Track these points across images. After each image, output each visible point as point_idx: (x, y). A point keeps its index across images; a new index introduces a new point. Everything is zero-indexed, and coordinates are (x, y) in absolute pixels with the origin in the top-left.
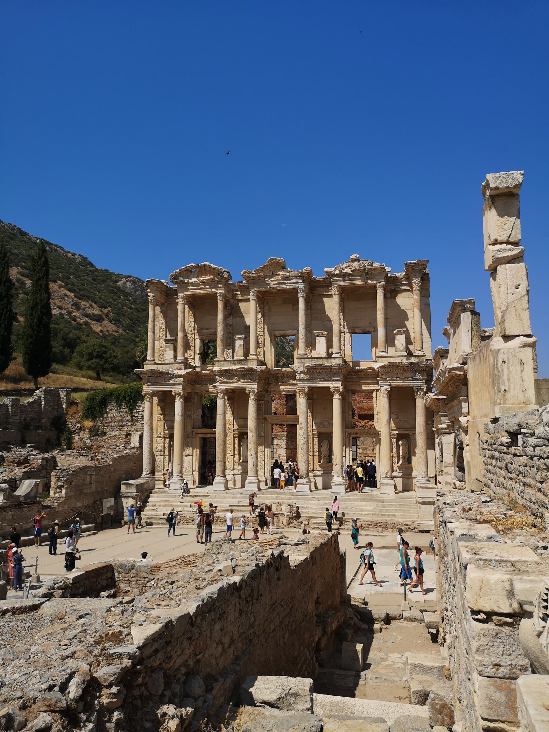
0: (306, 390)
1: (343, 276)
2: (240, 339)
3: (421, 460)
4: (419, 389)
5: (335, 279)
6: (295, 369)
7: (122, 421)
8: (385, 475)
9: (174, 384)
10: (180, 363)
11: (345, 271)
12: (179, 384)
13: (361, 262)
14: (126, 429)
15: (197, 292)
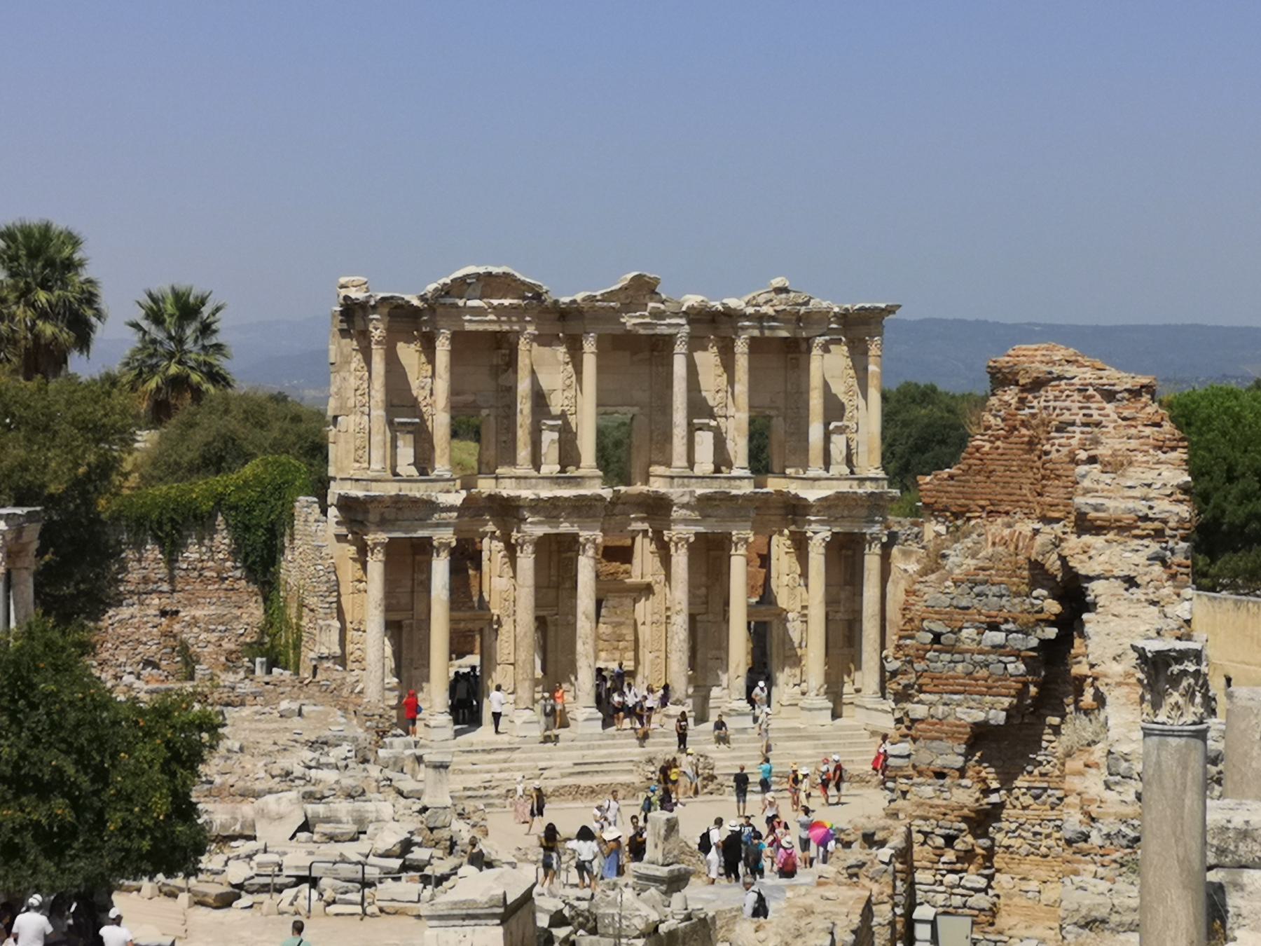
0: (692, 540)
1: (760, 318)
2: (552, 428)
3: (872, 664)
4: (875, 538)
5: (747, 323)
6: (673, 497)
7: (146, 580)
8: (815, 692)
9: (438, 525)
10: (448, 480)
11: (766, 309)
12: (447, 525)
13: (792, 295)
14: (156, 601)
15: (481, 328)
